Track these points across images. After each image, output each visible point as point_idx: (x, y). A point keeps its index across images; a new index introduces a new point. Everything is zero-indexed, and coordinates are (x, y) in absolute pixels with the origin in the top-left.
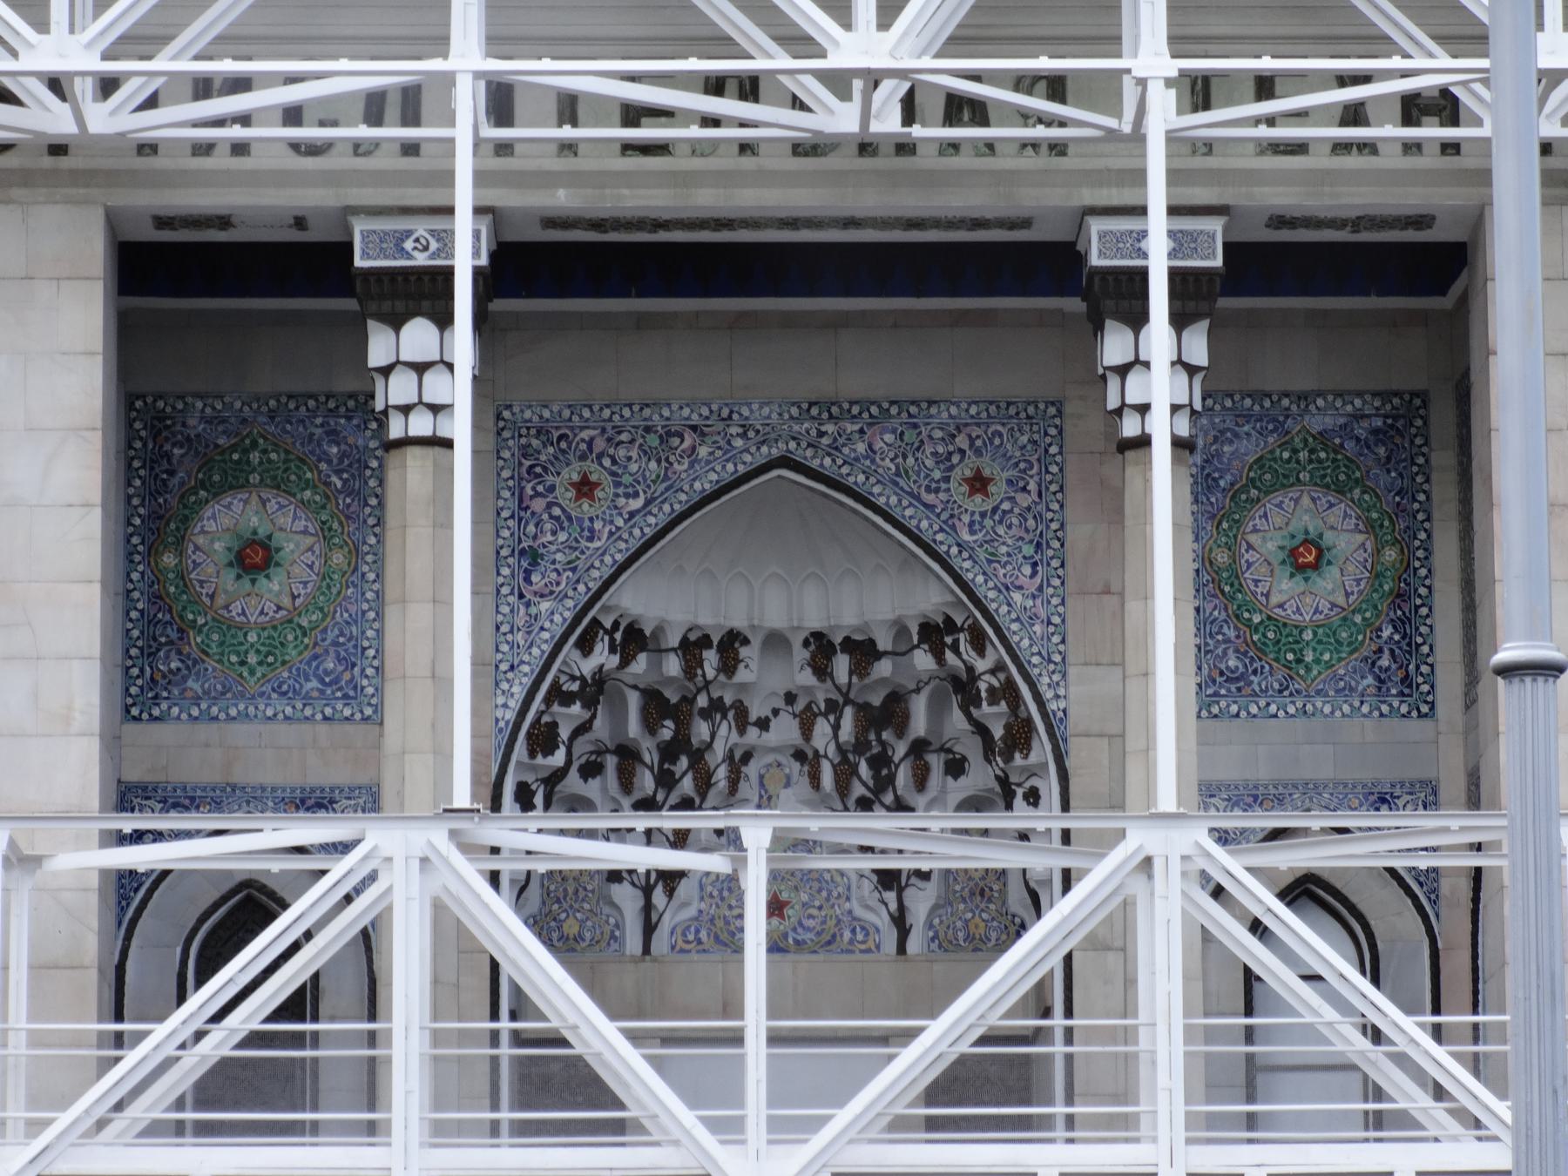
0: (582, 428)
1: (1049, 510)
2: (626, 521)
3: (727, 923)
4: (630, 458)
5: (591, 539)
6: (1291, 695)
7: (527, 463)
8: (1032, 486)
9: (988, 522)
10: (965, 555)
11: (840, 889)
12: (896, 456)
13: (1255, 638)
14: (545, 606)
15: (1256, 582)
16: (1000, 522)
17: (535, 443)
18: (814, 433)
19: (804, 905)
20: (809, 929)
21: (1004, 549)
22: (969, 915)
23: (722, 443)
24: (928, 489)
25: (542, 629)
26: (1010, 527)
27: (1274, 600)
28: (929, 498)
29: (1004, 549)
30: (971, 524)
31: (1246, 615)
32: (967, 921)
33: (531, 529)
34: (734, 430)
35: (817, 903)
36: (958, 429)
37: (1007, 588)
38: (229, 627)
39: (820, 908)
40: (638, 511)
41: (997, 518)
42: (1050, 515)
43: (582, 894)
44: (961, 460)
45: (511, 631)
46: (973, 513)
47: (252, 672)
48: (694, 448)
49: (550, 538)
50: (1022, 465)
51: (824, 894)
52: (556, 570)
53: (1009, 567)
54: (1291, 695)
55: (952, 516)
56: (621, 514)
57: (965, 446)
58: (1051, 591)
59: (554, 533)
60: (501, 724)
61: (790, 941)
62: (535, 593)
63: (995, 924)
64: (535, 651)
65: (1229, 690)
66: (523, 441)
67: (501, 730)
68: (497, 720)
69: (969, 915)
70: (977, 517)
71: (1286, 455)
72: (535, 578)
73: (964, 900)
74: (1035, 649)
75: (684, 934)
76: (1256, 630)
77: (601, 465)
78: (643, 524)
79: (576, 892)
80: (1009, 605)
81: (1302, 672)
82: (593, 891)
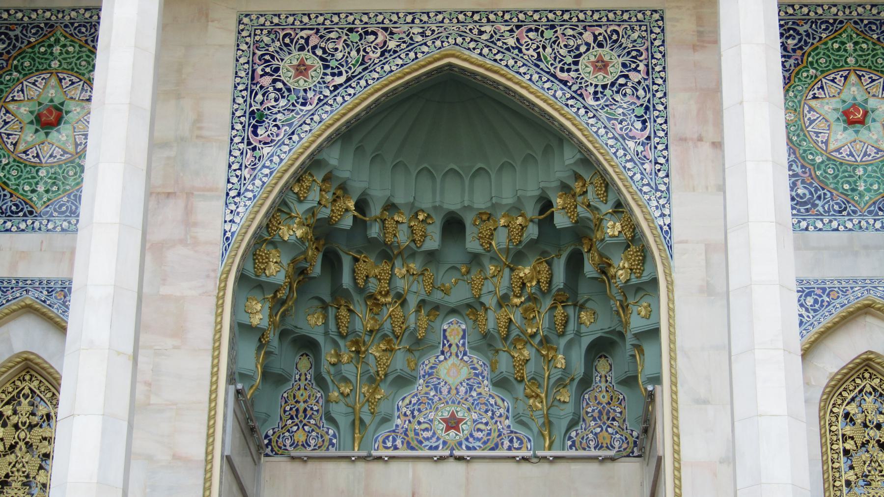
0: (302, 29)
1: (654, 83)
2: (331, 92)
3: (417, 434)
4: (336, 49)
5: (304, 104)
6: (849, 214)
7: (259, 53)
8: (642, 67)
9: (608, 92)
10: (590, 114)
11: (502, 411)
12: (538, 47)
13: (818, 173)
14: (267, 150)
15: (817, 134)
16: (618, 92)
17: (267, 40)
18: (475, 31)
19: (474, 421)
20: (479, 440)
21: (620, 111)
22: (599, 430)
23: (407, 39)
24: (562, 70)
25: (264, 166)
26: (625, 95)
27: (832, 147)
28: (564, 76)
29: (620, 111)
30: (596, 93)
31: (810, 157)
32: (596, 434)
33: (260, 97)
34: (416, 30)
35: (484, 421)
36: (585, 28)
37: (624, 139)
38: (25, 166)
39: (487, 424)
40: (341, 85)
41: (615, 89)
42: (655, 87)
43: (309, 413)
44: (588, 50)
45: (240, 169)
46: (596, 86)
47: (40, 197)
48: (385, 42)
49: (274, 104)
50: (634, 53)
51: (490, 414)
52: (276, 125)
53: (624, 123)
54: (849, 214)
55: (580, 88)
56: (328, 87)
57: (590, 40)
58: (657, 140)
59: (276, 100)
60: (228, 234)
61: (464, 447)
62: (260, 142)
63: (618, 436)
64: (258, 183)
65: (799, 211)
66: (258, 38)
67: (227, 239)
68: (225, 232)
69: (599, 430)
70: (599, 89)
71: (836, 46)
72: (260, 131)
73: (594, 419)
74: (645, 181)
75: (384, 442)
76: (819, 168)
77: (314, 53)
78: (344, 94)
79: (305, 410)
80: (624, 149)
81: (856, 198)
82: (317, 411)
